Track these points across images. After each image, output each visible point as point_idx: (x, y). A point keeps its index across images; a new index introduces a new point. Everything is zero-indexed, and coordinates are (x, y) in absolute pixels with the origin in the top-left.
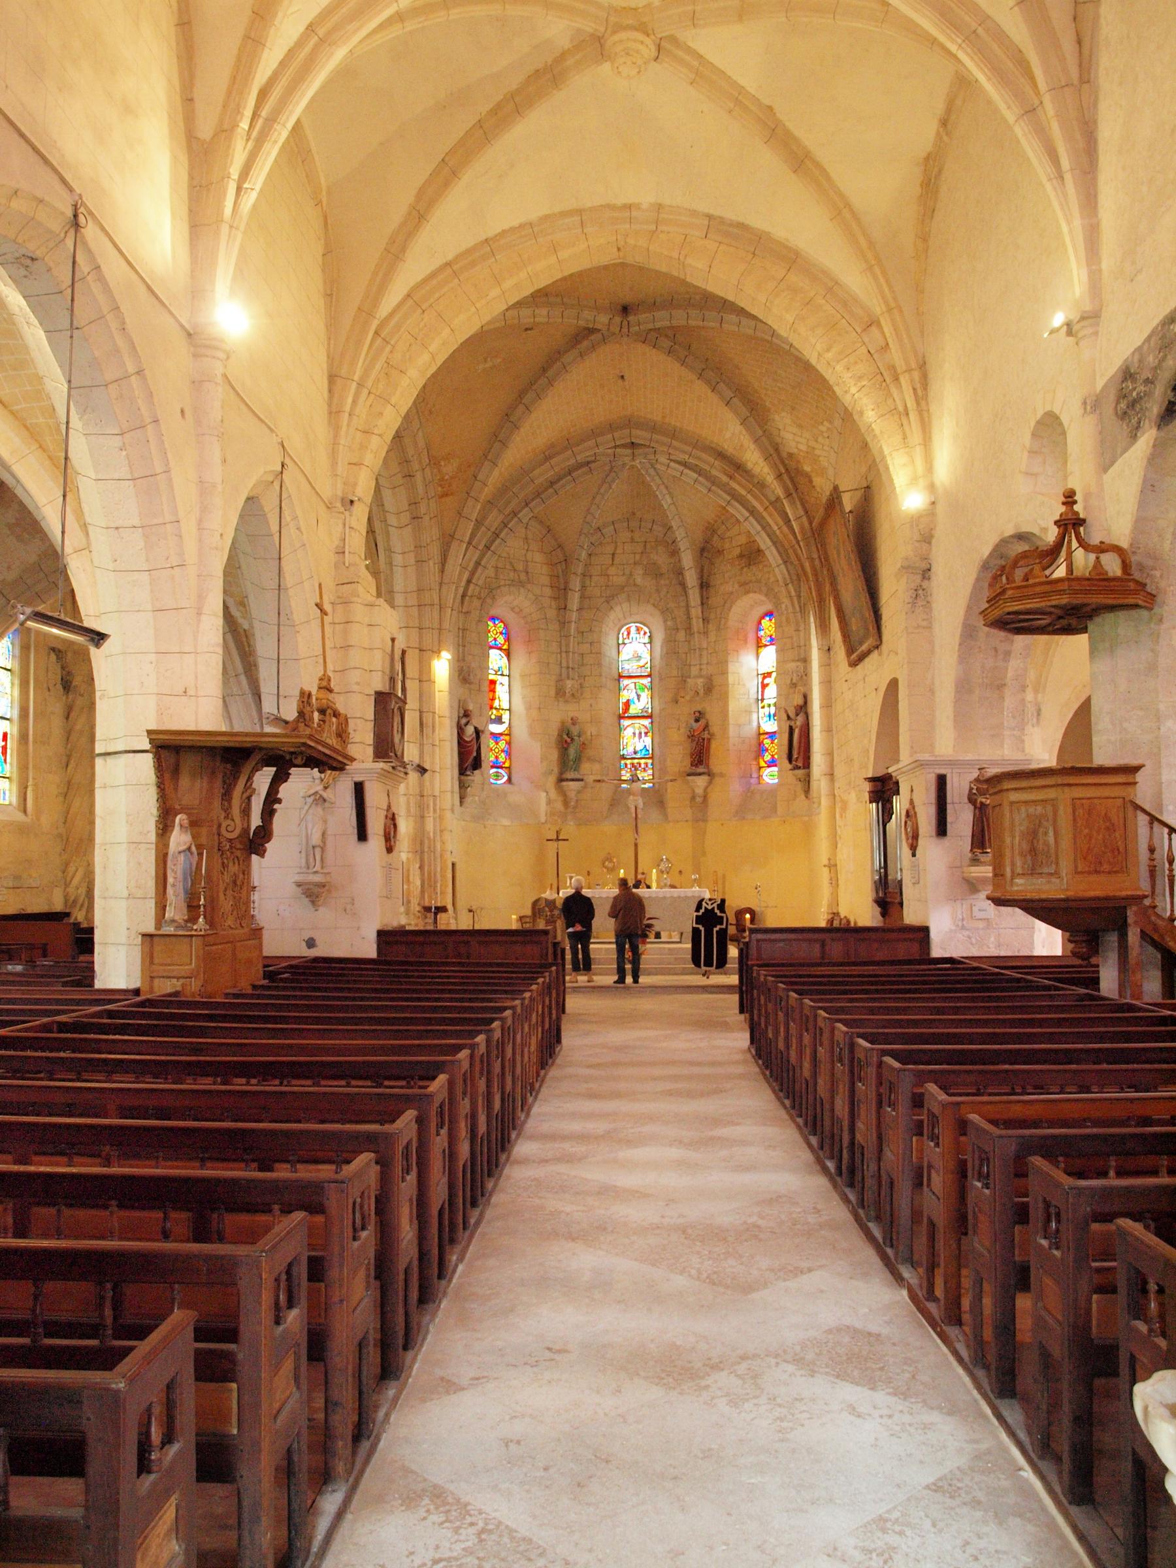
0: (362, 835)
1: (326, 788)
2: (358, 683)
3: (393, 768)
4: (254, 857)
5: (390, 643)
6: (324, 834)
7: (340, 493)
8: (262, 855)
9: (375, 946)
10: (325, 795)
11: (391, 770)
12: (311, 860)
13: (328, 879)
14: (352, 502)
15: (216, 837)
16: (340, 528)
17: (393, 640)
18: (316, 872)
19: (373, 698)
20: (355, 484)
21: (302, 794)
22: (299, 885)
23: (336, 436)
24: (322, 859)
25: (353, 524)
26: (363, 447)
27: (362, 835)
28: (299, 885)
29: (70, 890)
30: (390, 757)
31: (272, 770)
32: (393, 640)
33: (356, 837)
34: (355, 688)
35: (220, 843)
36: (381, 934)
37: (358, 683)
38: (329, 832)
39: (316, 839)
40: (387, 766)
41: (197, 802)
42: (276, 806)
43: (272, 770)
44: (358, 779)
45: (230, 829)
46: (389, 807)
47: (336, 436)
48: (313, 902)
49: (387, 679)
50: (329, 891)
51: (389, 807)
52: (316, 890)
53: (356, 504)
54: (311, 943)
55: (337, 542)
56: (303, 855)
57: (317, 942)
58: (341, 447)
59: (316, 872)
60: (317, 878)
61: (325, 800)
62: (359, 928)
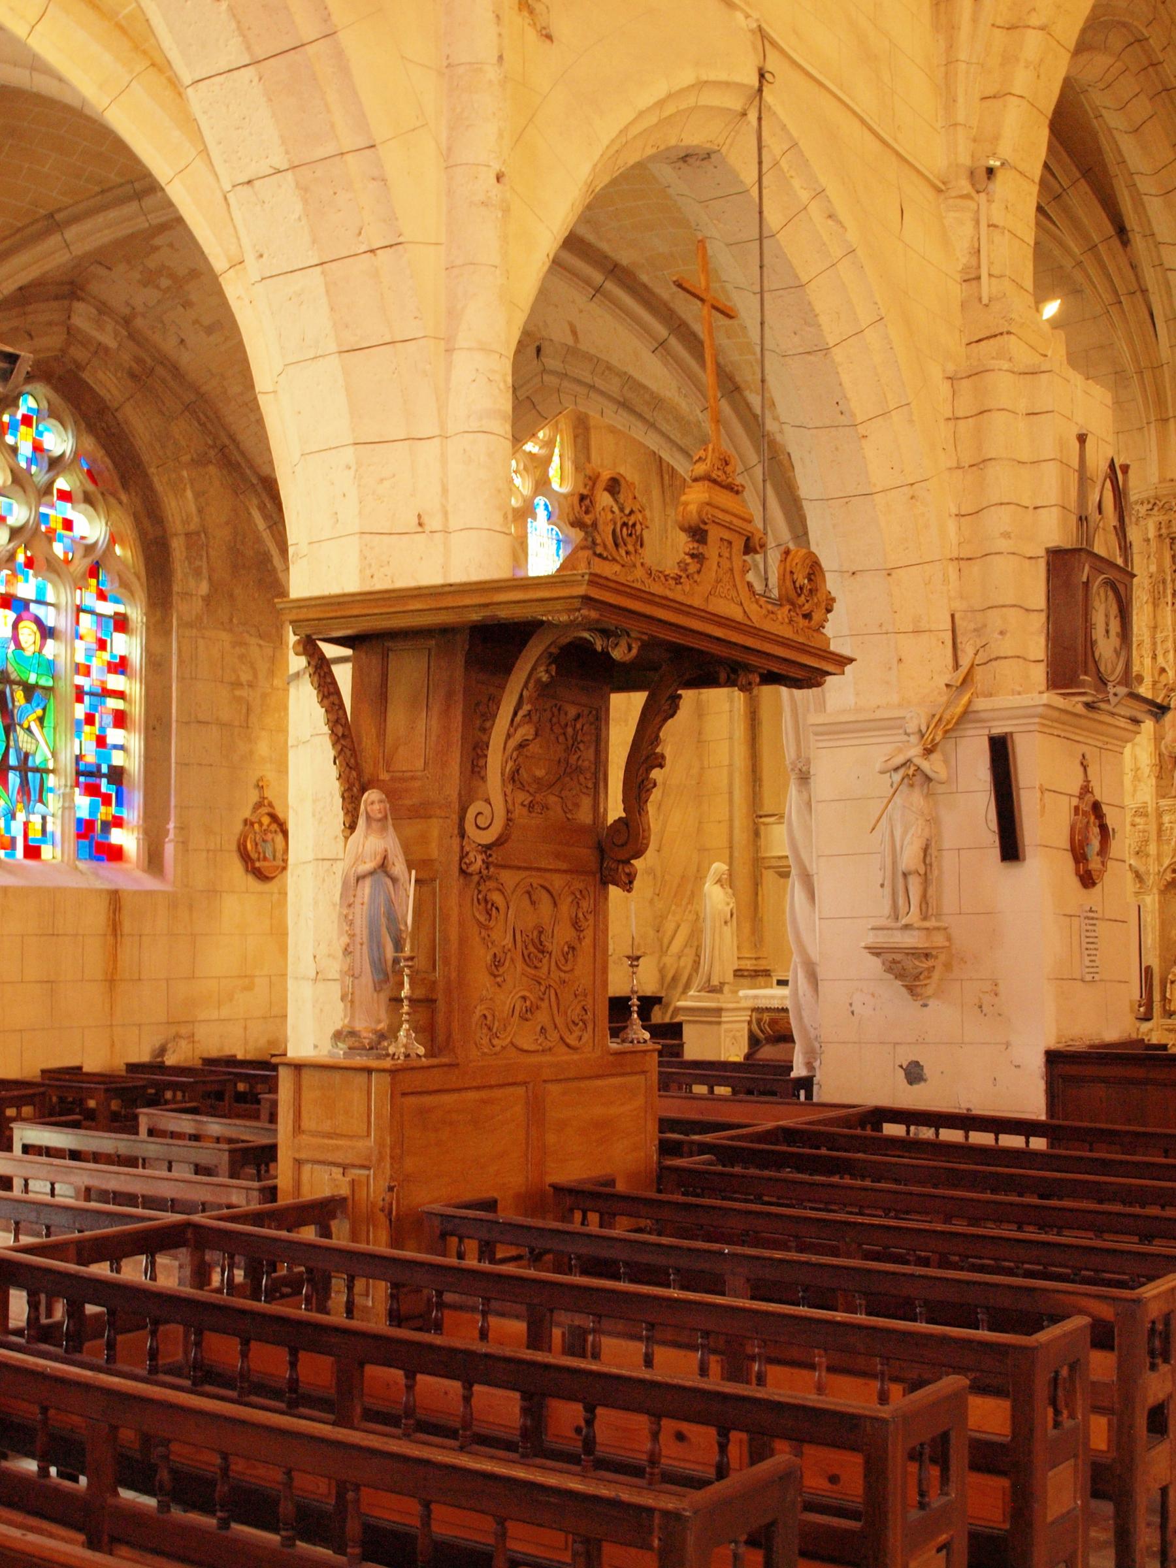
0: (1011, 849)
1: (928, 752)
2: (1006, 535)
3: (1089, 706)
4: (614, 891)
5: (1076, 445)
6: (926, 850)
7: (965, 160)
8: (628, 884)
9: (1042, 1085)
10: (925, 765)
11: (1080, 709)
12: (901, 901)
13: (939, 940)
14: (990, 171)
15: (456, 841)
16: (968, 229)
17: (1082, 439)
18: (907, 927)
19: (1042, 565)
20: (996, 138)
21: (878, 766)
22: (876, 951)
23: (950, 47)
24: (924, 897)
25: (998, 216)
26: (1008, 59)
27: (1011, 849)
28: (876, 951)
29: (668, 960)
30: (1082, 684)
31: (638, 699)
32: (1082, 439)
33: (996, 852)
34: (1003, 545)
35: (463, 855)
36: (1053, 1058)
37: (1006, 535)
38: (949, 840)
39: (910, 857)
40: (1076, 704)
41: (420, 764)
42: (655, 774)
43: (638, 699)
44: (997, 731)
45: (482, 822)
46: (1086, 790)
47: (950, 47)
48: (911, 989)
49: (1073, 519)
50: (948, 966)
51: (1086, 790)
52: (909, 963)
53: (1000, 176)
54: (914, 1073)
55: (963, 258)
56: (887, 890)
57: (927, 1071)
58: (962, 67)
59: (907, 927)
60: (910, 940)
61: (928, 779)
62: (1008, 1045)
